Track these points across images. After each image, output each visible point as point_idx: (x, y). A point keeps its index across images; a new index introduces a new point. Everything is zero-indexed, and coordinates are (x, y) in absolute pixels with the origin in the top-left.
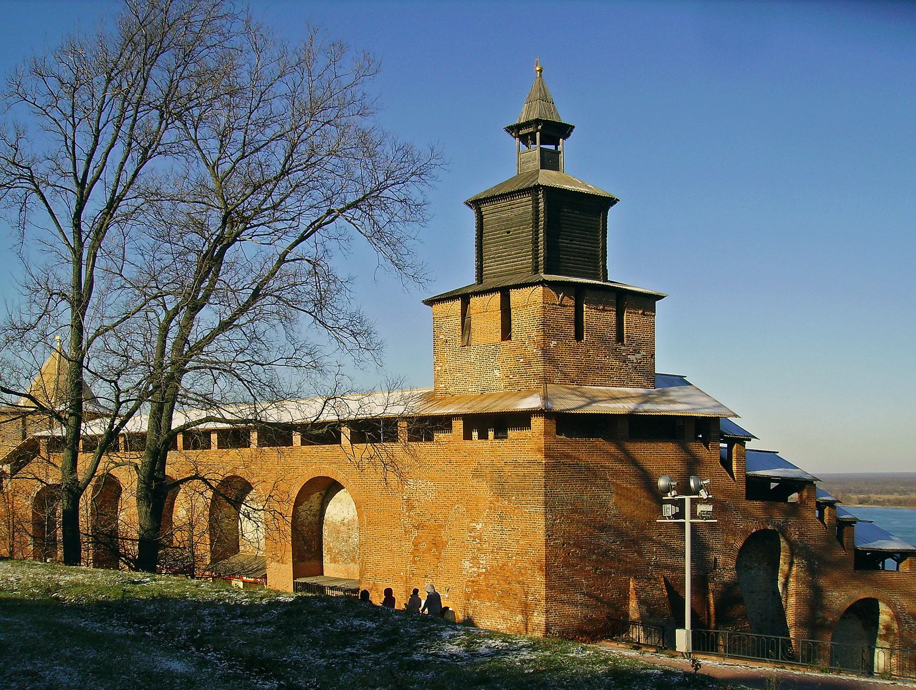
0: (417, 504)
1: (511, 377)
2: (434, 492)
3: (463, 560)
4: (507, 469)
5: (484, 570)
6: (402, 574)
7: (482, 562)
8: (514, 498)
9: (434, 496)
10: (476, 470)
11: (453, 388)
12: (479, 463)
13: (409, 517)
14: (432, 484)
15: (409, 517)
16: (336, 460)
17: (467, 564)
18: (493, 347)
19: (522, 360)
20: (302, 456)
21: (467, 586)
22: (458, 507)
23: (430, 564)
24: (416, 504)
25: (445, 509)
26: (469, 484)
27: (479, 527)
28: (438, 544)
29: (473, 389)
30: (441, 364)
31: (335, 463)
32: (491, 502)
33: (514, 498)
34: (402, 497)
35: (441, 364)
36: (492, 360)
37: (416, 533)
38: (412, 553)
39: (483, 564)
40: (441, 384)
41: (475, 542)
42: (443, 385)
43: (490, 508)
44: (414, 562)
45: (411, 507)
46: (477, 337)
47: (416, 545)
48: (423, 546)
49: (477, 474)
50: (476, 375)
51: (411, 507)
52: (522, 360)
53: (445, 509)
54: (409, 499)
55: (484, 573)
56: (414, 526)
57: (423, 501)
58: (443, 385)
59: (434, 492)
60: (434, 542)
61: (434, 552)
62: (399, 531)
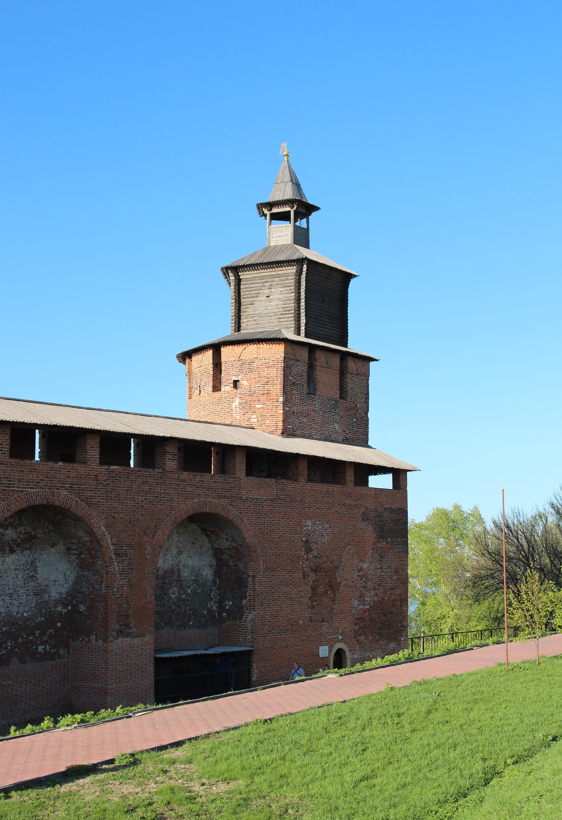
0: (314, 546)
1: (347, 432)
2: (330, 534)
3: (353, 599)
4: (386, 514)
5: (368, 606)
6: (301, 622)
7: (367, 599)
8: (389, 540)
9: (330, 538)
10: (364, 513)
11: (300, 432)
12: (366, 508)
13: (307, 560)
14: (328, 526)
15: (307, 560)
16: (228, 494)
17: (356, 603)
18: (334, 402)
19: (355, 420)
20: (178, 485)
21: (355, 624)
22: (349, 548)
23: (326, 607)
24: (314, 546)
25: (339, 550)
26: (358, 527)
27: (365, 566)
28: (333, 586)
29: (317, 436)
30: (289, 405)
31: (225, 497)
32: (374, 544)
33: (389, 540)
34: (301, 539)
35: (289, 405)
36: (333, 414)
37: (312, 577)
38: (310, 598)
39: (367, 601)
40: (289, 425)
41: (362, 581)
42: (291, 427)
43: (373, 549)
44: (313, 607)
45: (309, 550)
46: (321, 389)
47: (314, 589)
48: (321, 589)
49: (365, 518)
50: (320, 424)
51: (309, 550)
52: (355, 420)
53: (339, 550)
54: (307, 541)
55: (368, 609)
56: (313, 570)
57: (320, 542)
58: (291, 427)
59: (330, 534)
60: (330, 584)
61: (330, 595)
62: (299, 575)
